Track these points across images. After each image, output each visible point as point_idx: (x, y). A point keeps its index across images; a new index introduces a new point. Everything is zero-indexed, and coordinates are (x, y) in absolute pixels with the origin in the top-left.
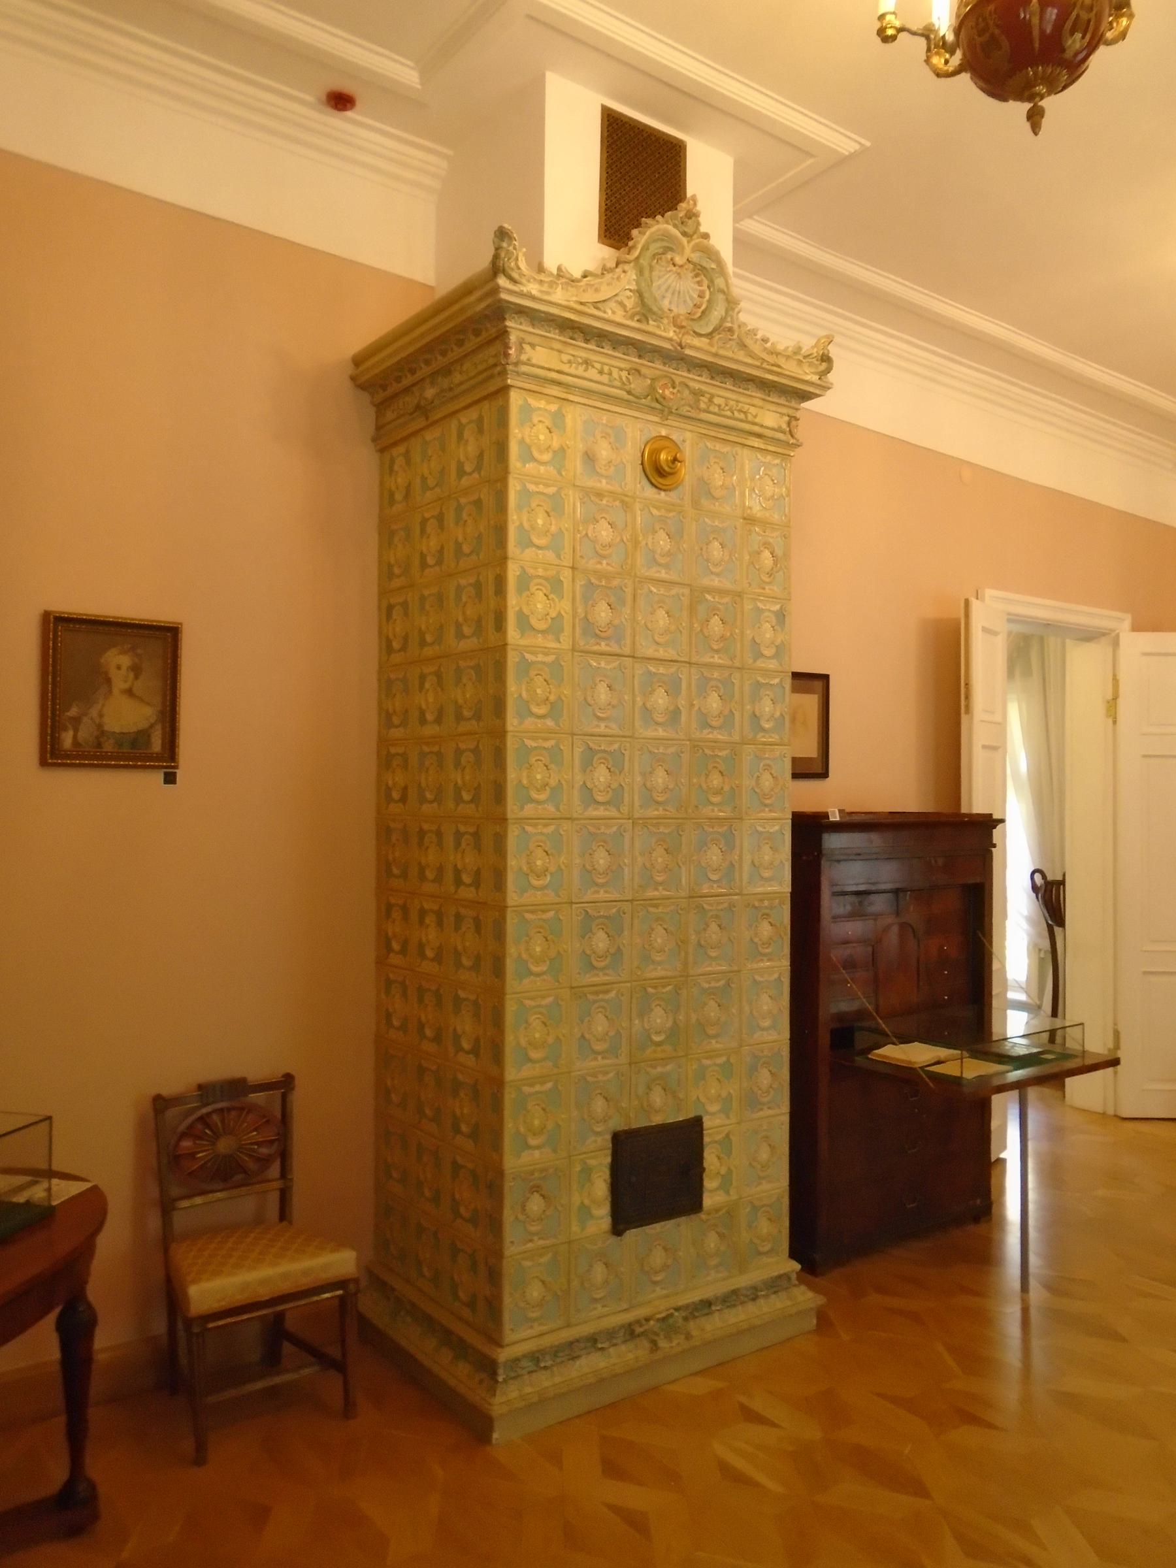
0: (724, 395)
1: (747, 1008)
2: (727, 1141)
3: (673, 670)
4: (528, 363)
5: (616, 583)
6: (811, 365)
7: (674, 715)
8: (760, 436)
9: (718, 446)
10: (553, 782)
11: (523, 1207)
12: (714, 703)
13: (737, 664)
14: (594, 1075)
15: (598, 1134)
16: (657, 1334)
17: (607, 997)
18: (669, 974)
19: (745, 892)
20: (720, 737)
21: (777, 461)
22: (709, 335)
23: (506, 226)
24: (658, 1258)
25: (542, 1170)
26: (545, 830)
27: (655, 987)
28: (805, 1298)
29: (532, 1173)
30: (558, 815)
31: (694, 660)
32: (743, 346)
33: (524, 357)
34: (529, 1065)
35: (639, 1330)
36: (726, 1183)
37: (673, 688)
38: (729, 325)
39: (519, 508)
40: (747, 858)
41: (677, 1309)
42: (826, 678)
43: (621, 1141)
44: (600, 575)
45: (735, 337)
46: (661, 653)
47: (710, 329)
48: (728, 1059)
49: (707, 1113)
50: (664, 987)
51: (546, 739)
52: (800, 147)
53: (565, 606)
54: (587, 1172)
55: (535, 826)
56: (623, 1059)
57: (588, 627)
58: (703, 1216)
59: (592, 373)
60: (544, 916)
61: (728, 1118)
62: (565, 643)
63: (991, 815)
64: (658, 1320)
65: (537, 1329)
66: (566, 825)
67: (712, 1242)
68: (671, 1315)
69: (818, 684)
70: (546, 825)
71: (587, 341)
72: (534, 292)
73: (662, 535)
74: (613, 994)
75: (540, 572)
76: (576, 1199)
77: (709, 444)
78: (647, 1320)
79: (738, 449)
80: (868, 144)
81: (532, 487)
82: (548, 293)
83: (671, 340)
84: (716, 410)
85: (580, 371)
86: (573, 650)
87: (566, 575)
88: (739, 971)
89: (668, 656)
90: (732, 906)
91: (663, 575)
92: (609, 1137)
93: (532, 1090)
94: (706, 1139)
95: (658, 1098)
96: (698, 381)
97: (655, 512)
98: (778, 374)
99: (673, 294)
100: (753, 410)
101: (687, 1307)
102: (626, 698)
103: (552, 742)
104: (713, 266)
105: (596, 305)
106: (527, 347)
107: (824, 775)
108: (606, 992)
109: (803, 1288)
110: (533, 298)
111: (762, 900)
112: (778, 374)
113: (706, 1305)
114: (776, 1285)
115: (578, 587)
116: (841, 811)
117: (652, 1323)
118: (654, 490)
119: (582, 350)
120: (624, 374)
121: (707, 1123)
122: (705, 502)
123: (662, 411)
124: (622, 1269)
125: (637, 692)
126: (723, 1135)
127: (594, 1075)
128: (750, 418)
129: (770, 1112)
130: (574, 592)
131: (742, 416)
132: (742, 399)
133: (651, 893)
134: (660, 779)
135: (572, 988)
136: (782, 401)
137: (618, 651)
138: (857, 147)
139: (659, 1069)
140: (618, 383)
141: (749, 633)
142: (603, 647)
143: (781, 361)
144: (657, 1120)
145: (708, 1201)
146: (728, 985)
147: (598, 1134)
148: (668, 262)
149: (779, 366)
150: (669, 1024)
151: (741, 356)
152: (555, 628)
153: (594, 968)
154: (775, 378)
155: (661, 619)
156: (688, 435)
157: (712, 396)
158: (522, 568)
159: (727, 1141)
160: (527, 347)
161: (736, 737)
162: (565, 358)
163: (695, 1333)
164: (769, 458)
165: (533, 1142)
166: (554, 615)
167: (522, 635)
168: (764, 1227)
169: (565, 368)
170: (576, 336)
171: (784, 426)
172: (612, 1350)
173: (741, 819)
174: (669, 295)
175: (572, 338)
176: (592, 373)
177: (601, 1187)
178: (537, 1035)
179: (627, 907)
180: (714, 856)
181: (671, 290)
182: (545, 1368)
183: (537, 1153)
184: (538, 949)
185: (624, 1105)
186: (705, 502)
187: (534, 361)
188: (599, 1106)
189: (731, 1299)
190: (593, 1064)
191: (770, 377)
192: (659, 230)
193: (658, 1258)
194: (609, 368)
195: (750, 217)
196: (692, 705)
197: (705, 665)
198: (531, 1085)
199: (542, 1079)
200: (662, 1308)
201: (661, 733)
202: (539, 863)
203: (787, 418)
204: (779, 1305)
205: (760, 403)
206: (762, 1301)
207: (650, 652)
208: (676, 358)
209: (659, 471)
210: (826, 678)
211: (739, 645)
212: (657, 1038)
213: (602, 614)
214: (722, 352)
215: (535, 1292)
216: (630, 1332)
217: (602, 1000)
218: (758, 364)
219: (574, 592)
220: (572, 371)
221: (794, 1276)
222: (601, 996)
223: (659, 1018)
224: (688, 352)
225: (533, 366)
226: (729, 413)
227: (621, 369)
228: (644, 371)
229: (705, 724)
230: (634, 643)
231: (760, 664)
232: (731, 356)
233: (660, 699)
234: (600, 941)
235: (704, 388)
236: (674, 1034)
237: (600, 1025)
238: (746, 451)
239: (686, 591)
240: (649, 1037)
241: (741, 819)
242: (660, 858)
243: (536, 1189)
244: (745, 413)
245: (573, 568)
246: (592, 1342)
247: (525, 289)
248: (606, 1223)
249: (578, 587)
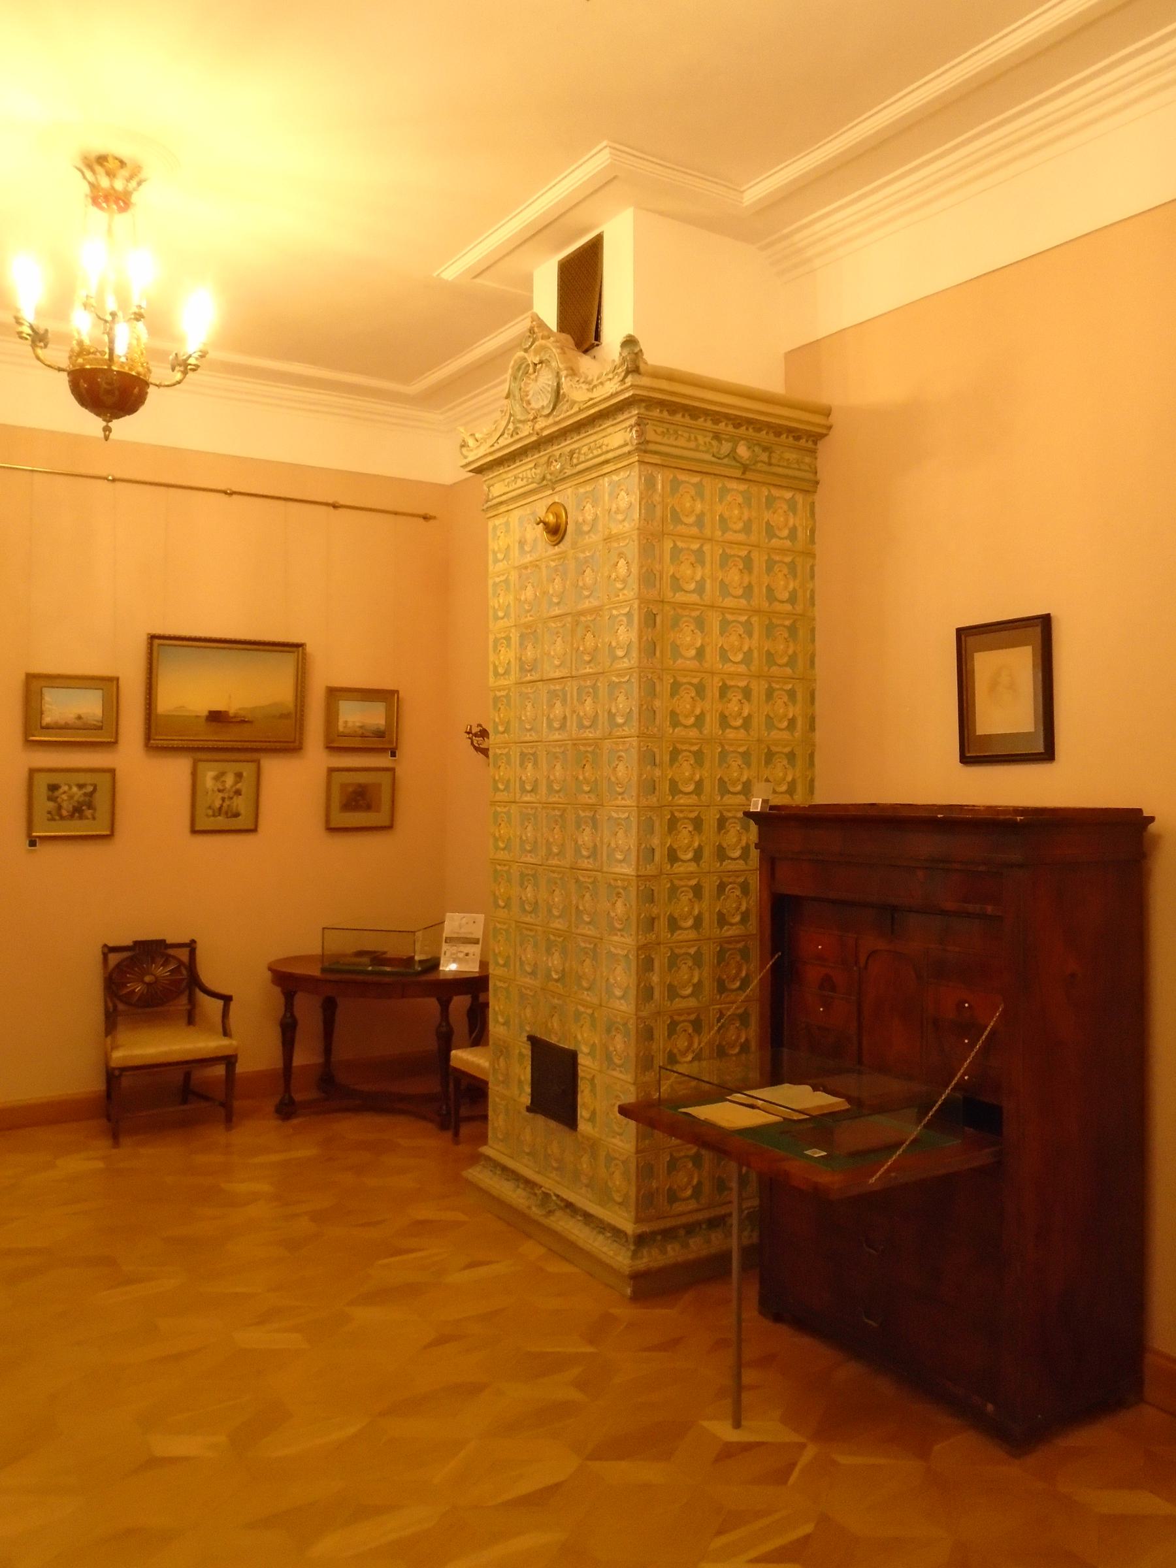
8: (607, 462)
19: (605, 869)
31: (574, 674)
42: (1045, 623)
63: (1140, 811)
71: (515, 462)
89: (562, 675)
96: (566, 446)
101: (562, 1200)
107: (1048, 754)
111: (616, 880)
116: (765, 802)
131: (600, 451)
157: (579, 448)
173: (602, 805)
191: (592, 411)
206: (601, 1237)
207: (552, 675)
209: (556, 532)
224: (545, 433)
241: (602, 805)
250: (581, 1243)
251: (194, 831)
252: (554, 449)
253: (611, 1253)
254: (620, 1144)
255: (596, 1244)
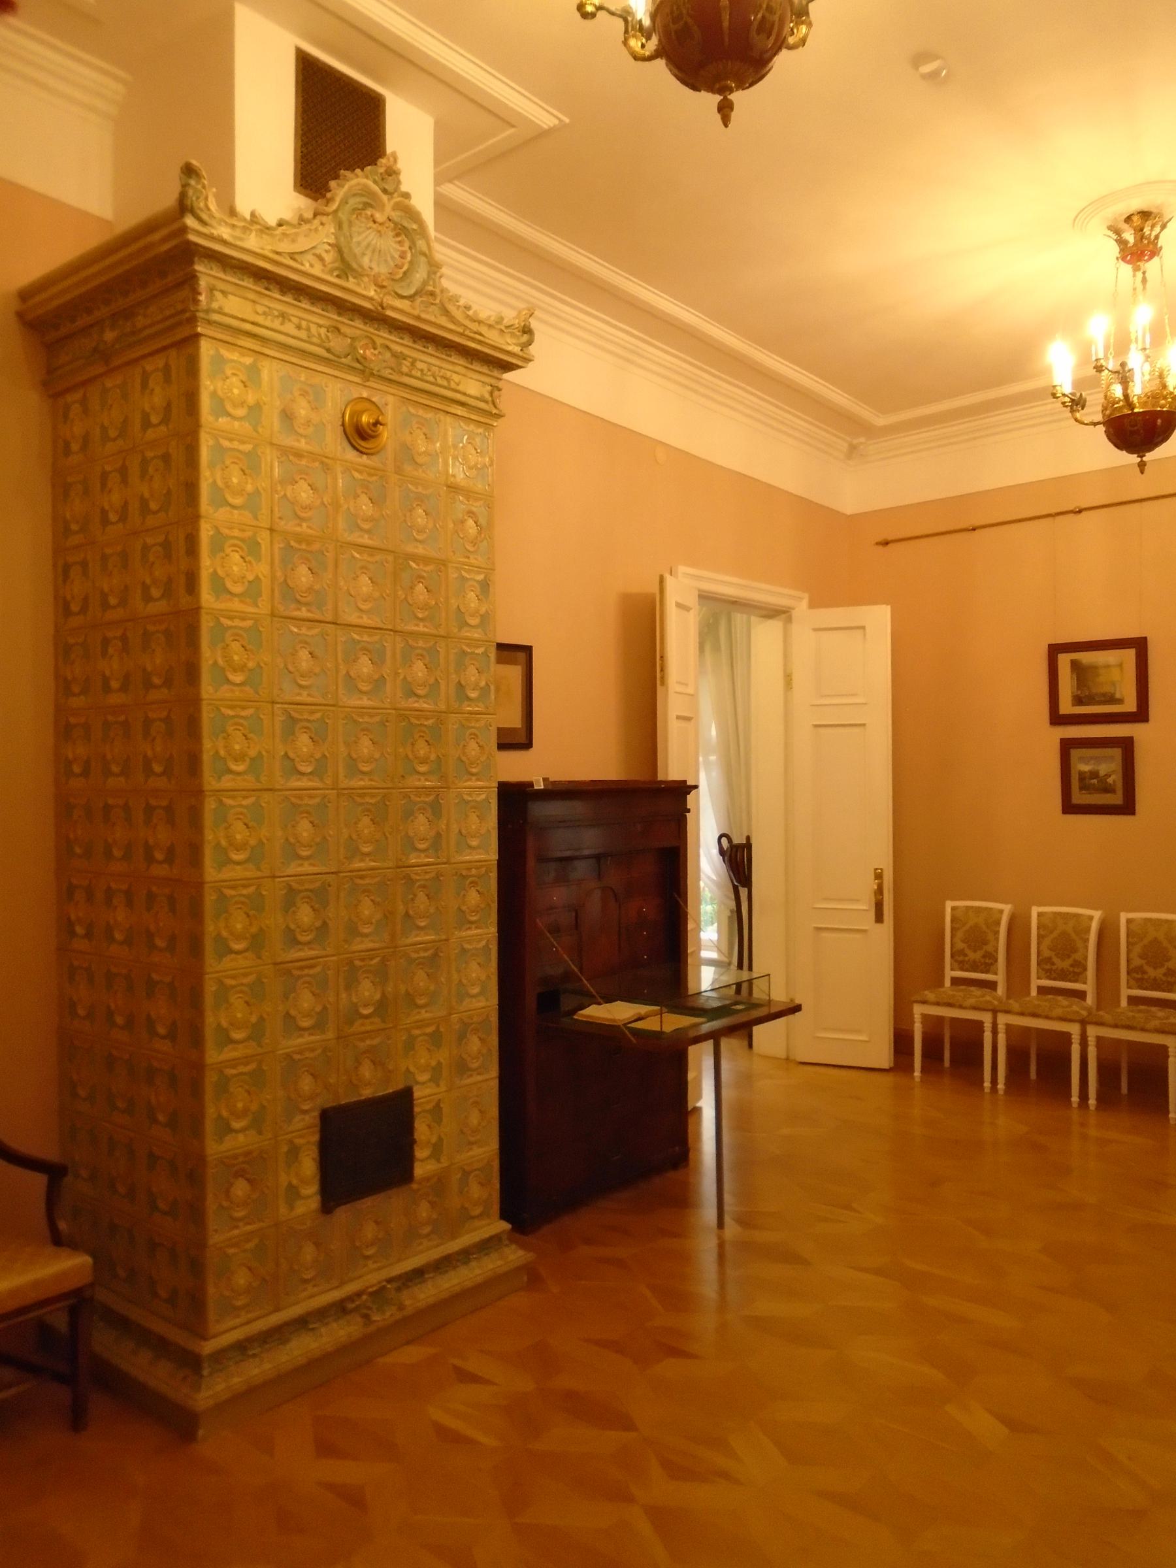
0: (427, 361)
1: (455, 976)
2: (437, 1111)
3: (377, 638)
4: (220, 311)
5: (316, 546)
6: (513, 335)
7: (379, 683)
8: (463, 404)
9: (421, 412)
10: (253, 753)
11: (228, 1192)
12: (419, 670)
13: (442, 632)
14: (300, 1053)
15: (305, 1112)
16: (370, 1308)
17: (311, 972)
18: (377, 945)
19: (453, 860)
20: (425, 705)
21: (480, 430)
22: (411, 298)
23: (194, 162)
24: (370, 1231)
25: (249, 1153)
26: (245, 802)
27: (363, 960)
28: (514, 1256)
29: (235, 1157)
30: (259, 786)
31: (399, 628)
32: (446, 312)
33: (215, 305)
34: (231, 1046)
35: (351, 1306)
36: (437, 1150)
37: (378, 659)
38: (430, 288)
39: (212, 466)
40: (455, 828)
41: (389, 1281)
42: (528, 650)
43: (328, 1117)
44: (300, 538)
45: (437, 301)
46: (365, 621)
47: (412, 291)
48: (438, 1027)
49: (417, 1083)
50: (371, 959)
51: (244, 708)
52: (500, 116)
53: (263, 569)
54: (294, 1152)
55: (233, 797)
56: (330, 1035)
57: (288, 591)
58: (415, 1186)
59: (289, 328)
60: (245, 892)
61: (438, 1086)
62: (264, 607)
64: (371, 1294)
65: (244, 1316)
66: (266, 796)
67: (424, 1211)
68: (384, 1287)
69: (521, 656)
70: (245, 797)
71: (283, 293)
72: (225, 236)
73: (364, 499)
74: (318, 969)
75: (236, 533)
76: (284, 1179)
77: (412, 410)
78: (359, 1294)
79: (441, 416)
80: (567, 121)
81: (226, 443)
82: (241, 239)
83: (371, 299)
84: (419, 374)
85: (276, 324)
86: (273, 615)
87: (264, 538)
88: (447, 940)
89: (373, 625)
90: (438, 875)
91: (365, 540)
92: (316, 1114)
93: (234, 1072)
94: (417, 1109)
95: (367, 1071)
96: (401, 344)
97: (356, 475)
98: (480, 342)
99: (374, 251)
100: (456, 377)
102: (329, 665)
103: (251, 711)
104: (415, 226)
105: (292, 256)
106: (218, 294)
107: (527, 745)
108: (311, 967)
109: (514, 1247)
110: (224, 242)
111: (469, 869)
112: (480, 342)
113: (418, 1274)
114: (486, 1246)
115: (276, 551)
116: (545, 780)
117: (364, 1297)
118: (355, 453)
119: (277, 302)
120: (323, 331)
121: (417, 1094)
122: (408, 468)
123: (363, 372)
124: (332, 1247)
125: (340, 661)
126: (433, 1104)
127: (300, 1053)
128: (453, 385)
129: (479, 1078)
130: (272, 555)
131: (445, 383)
132: (444, 365)
133: (358, 865)
134: (365, 747)
135: (275, 964)
136: (485, 369)
137: (318, 616)
138: (556, 122)
139: (368, 1042)
140: (315, 340)
141: (454, 602)
142: (304, 613)
143: (484, 330)
144: (367, 1093)
145: (419, 1171)
146: (436, 955)
147: (305, 1112)
148: (367, 218)
149: (480, 334)
150: (378, 996)
151: (443, 321)
152: (252, 591)
153: (299, 943)
154: (478, 347)
155: (365, 585)
156: (390, 399)
158: (216, 528)
159: (437, 1111)
160: (218, 294)
161: (443, 707)
162: (260, 309)
163: (407, 1302)
164: (472, 427)
165: (236, 1125)
166: (251, 578)
167: (217, 598)
168: (476, 1191)
169: (260, 319)
170: (271, 287)
171: (487, 396)
172: (323, 1330)
174: (369, 253)
175: (267, 289)
176: (289, 328)
177: (309, 1165)
178: (239, 1015)
179: (330, 878)
180: (421, 825)
181: (371, 249)
182: (254, 1356)
183: (241, 1137)
184: (239, 926)
185: (331, 1081)
186: (408, 468)
187: (226, 310)
188: (306, 1084)
189: (443, 1265)
190: (300, 1040)
191: (473, 345)
192: (358, 184)
193: (370, 1231)
194: (305, 324)
195: (450, 181)
196: (397, 674)
197: (411, 633)
198: (234, 1067)
199: (246, 1060)
200: (375, 1281)
201: (365, 702)
202: (238, 837)
203: (489, 388)
204: (491, 1266)
205: (463, 371)
206: (473, 1264)
207: (353, 618)
208: (375, 317)
210: (528, 650)
211: (444, 614)
212: (365, 1012)
213: (303, 577)
214: (424, 316)
215: (242, 1279)
216: (340, 1309)
217: (308, 975)
218: (460, 330)
219: (272, 555)
220: (268, 323)
221: (505, 1237)
222: (306, 971)
223: (367, 990)
224: (389, 313)
225: (226, 315)
226: (431, 379)
227: (320, 326)
228: (344, 329)
229: (411, 693)
230: (336, 608)
231: (466, 633)
232: (432, 319)
233: (365, 666)
234: (305, 915)
235: (406, 351)
236: (382, 1007)
237: (306, 1000)
238: (449, 419)
239: (390, 558)
240: (357, 1012)
242: (365, 825)
243: (241, 1174)
244: (448, 380)
245: (271, 530)
246: (302, 1323)
247: (215, 232)
248: (314, 1203)
249: (276, 551)
250: (469, 1284)
251: (1069, 808)
252: (384, 336)
253: (499, 1263)
254: (481, 1150)
255: (478, 1271)
